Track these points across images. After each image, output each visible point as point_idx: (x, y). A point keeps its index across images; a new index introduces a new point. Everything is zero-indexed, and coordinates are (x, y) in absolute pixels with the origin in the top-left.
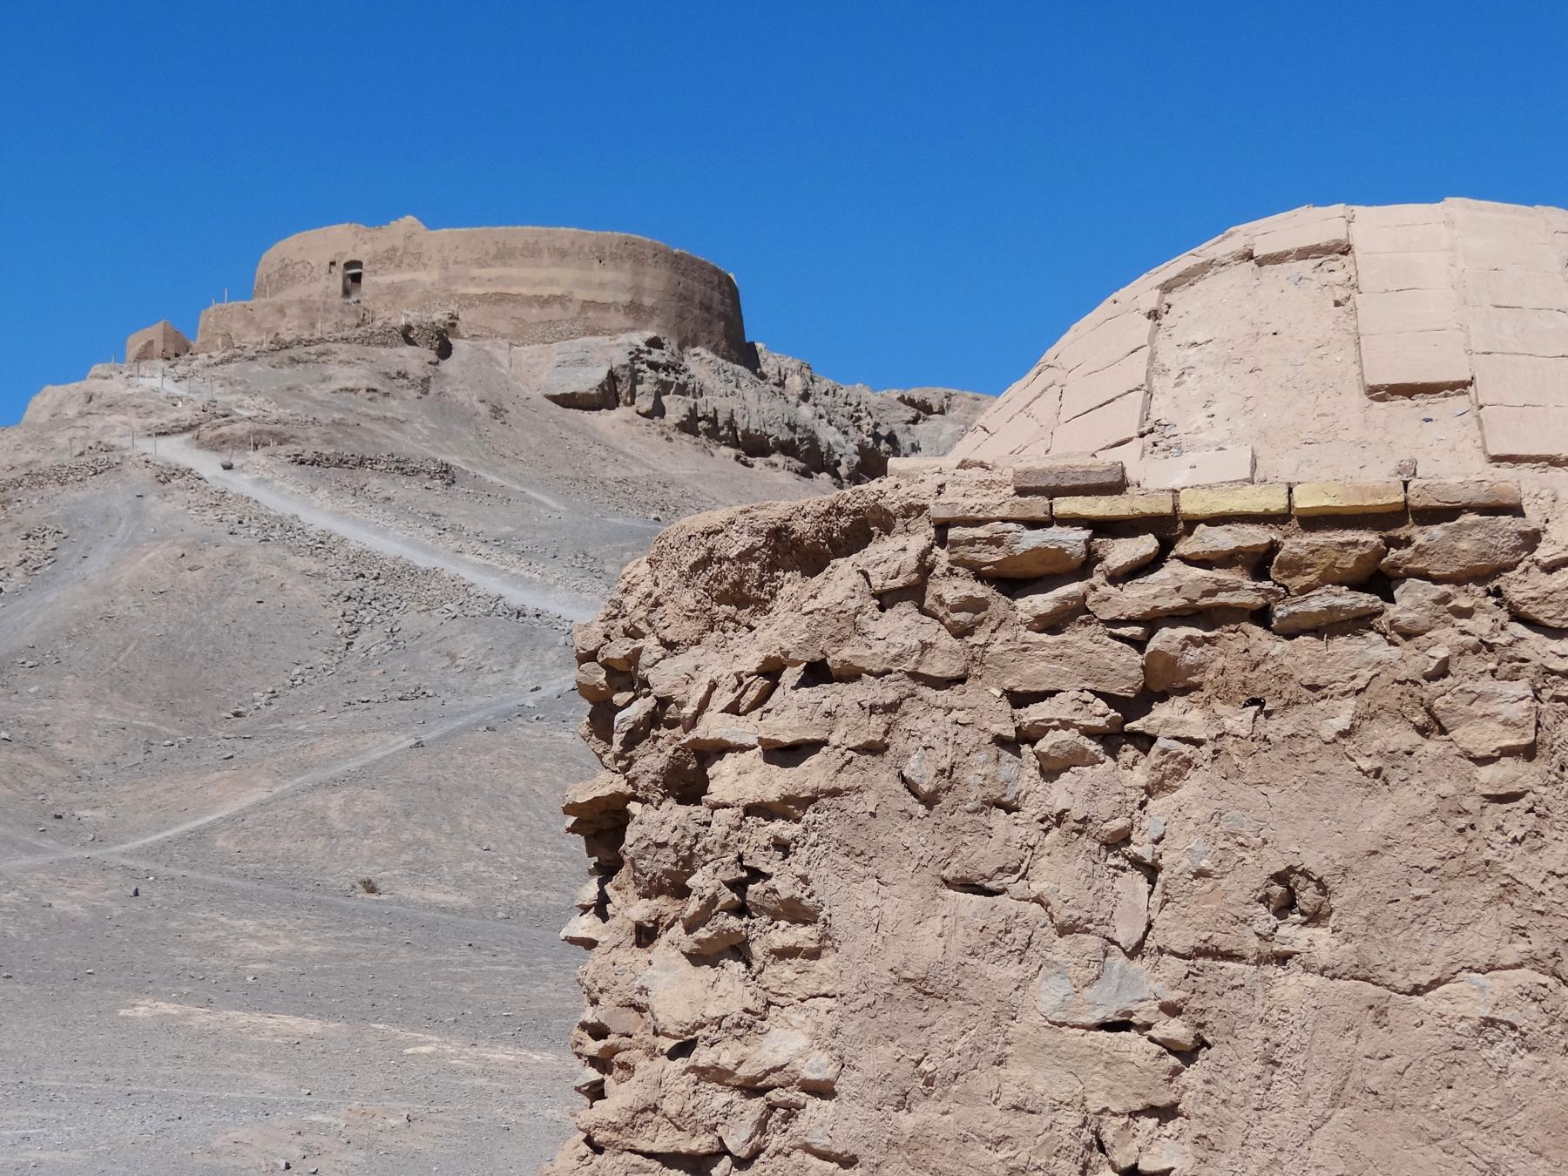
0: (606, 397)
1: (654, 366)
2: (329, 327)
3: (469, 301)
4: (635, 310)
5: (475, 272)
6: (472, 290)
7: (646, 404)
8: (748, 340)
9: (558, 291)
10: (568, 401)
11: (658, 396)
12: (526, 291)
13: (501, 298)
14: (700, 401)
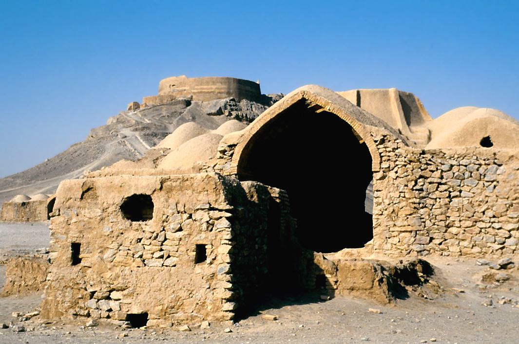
0: (220, 112)
1: (230, 105)
2: (165, 101)
3: (194, 93)
4: (229, 93)
5: (196, 87)
6: (196, 91)
7: (227, 114)
8: (262, 94)
9: (212, 90)
10: (209, 114)
11: (229, 112)
12: (206, 91)
13: (201, 92)
14: (239, 112)
